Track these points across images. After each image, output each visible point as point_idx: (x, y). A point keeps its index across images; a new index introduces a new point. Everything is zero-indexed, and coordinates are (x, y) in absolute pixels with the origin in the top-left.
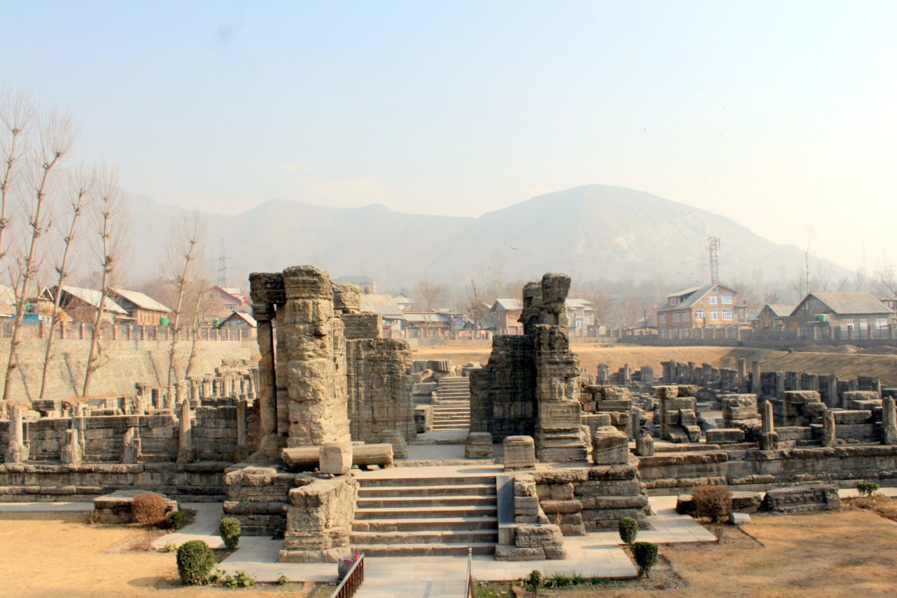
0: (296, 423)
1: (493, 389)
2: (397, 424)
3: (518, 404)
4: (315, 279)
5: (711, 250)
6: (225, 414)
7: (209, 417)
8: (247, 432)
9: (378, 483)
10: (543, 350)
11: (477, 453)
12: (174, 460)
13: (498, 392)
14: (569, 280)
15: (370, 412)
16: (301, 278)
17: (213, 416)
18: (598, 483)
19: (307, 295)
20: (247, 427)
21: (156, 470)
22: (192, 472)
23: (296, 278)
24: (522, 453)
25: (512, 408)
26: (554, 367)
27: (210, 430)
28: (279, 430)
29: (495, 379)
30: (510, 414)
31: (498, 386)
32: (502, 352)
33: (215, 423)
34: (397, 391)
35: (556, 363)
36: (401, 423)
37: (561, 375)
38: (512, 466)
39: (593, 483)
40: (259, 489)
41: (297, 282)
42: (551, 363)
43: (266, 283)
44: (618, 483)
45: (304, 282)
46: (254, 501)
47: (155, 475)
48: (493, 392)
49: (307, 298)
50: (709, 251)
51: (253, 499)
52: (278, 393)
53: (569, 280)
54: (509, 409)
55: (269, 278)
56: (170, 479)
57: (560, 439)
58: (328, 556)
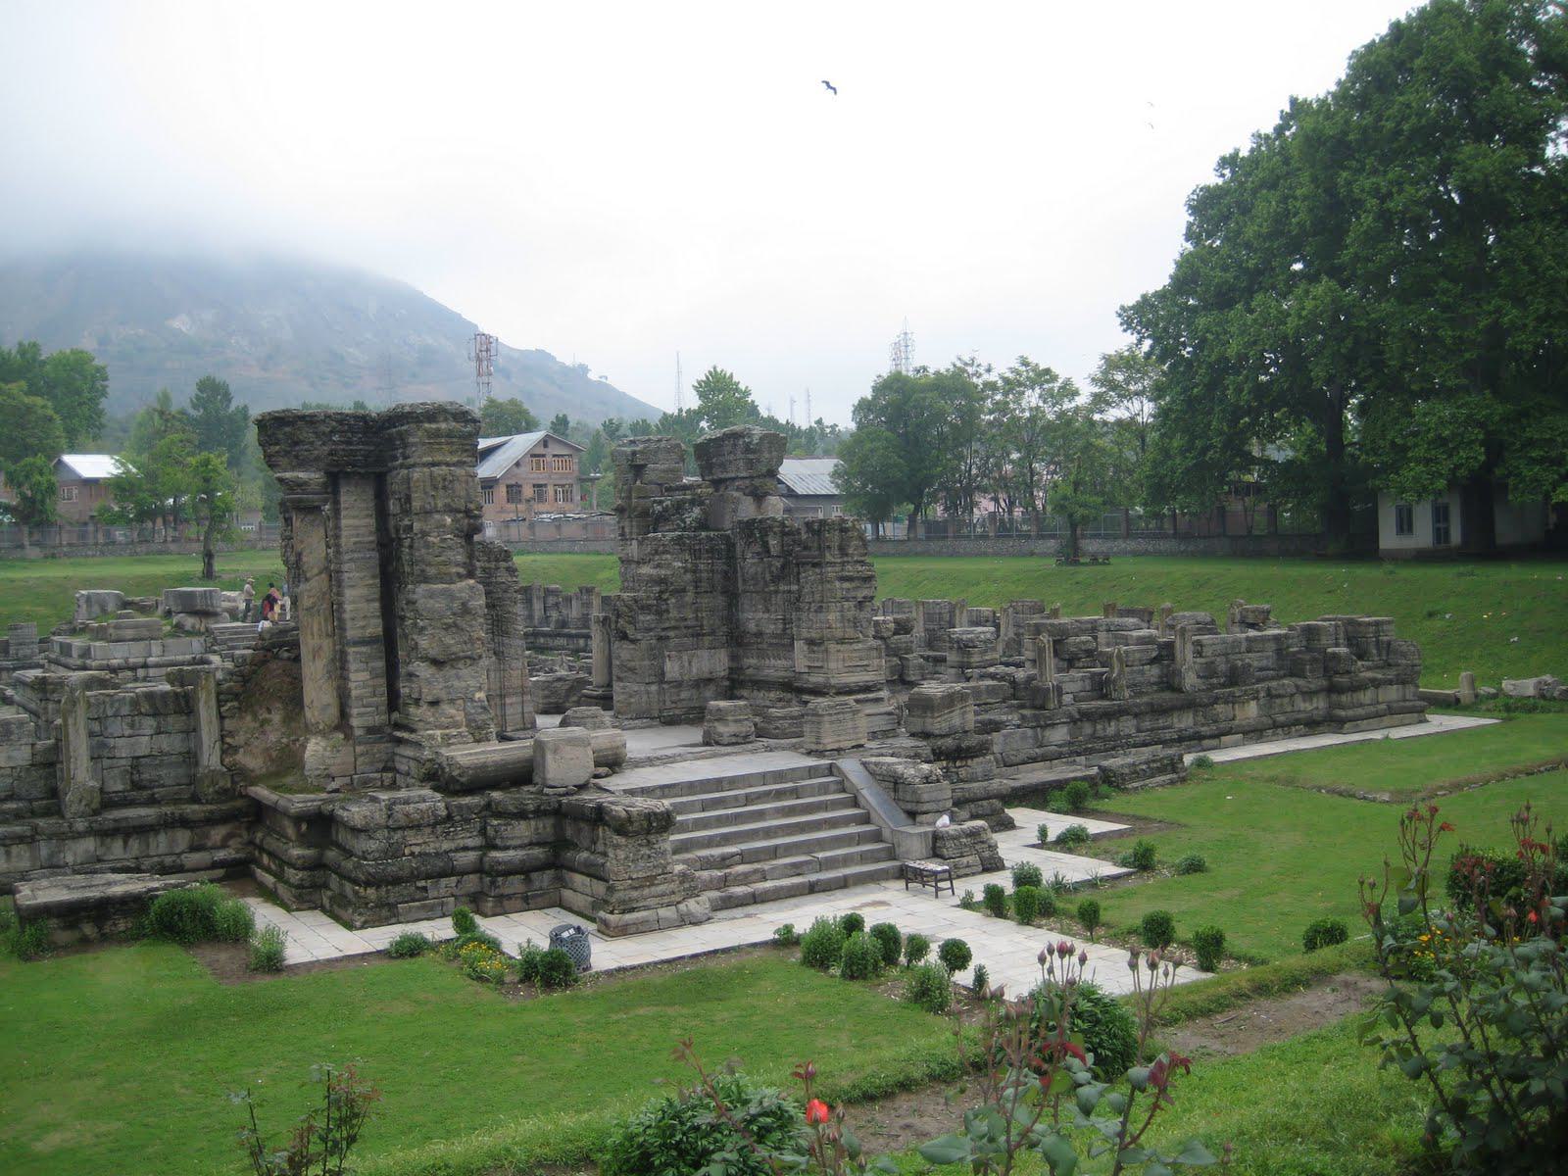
1: (664, 629)
2: (508, 701)
4: (469, 428)
5: (479, 360)
6: (153, 705)
7: (115, 716)
8: (222, 738)
9: (658, 792)
10: (829, 558)
12: (55, 809)
13: (671, 634)
16: (443, 426)
17: (125, 710)
19: (455, 459)
21: (20, 839)
22: (105, 834)
23: (434, 426)
24: (850, 724)
26: (846, 585)
27: (121, 742)
28: (355, 722)
30: (690, 671)
33: (132, 726)
36: (514, 699)
38: (835, 746)
40: (428, 830)
41: (437, 434)
42: (843, 579)
43: (333, 432)
45: (450, 434)
46: (420, 854)
47: (15, 850)
49: (454, 465)
50: (474, 364)
51: (417, 850)
55: (341, 422)
56: (51, 855)
58: (690, 914)
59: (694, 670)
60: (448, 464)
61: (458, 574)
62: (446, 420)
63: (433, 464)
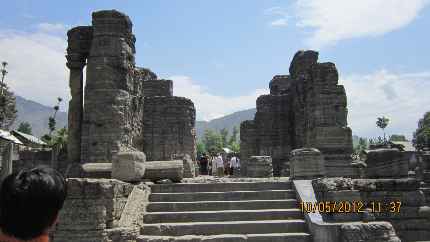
0: (95, 144)
1: (260, 136)
3: (280, 147)
7: (29, 159)
9: (171, 188)
11: (260, 172)
13: (263, 138)
14: (317, 54)
15: (162, 153)
18: (385, 193)
19: (112, 33)
20: (59, 164)
24: (313, 162)
25: (275, 151)
26: (326, 96)
29: (261, 128)
31: (263, 133)
32: (266, 108)
34: (184, 137)
35: (329, 93)
37: (332, 103)
39: (381, 193)
42: (324, 93)
43: (79, 34)
44: (404, 193)
48: (259, 138)
52: (83, 125)
53: (317, 54)
54: (273, 151)
57: (334, 158)
59: (275, 155)
60: (108, 36)
61: (110, 84)
62: (108, 17)
63: (102, 35)
